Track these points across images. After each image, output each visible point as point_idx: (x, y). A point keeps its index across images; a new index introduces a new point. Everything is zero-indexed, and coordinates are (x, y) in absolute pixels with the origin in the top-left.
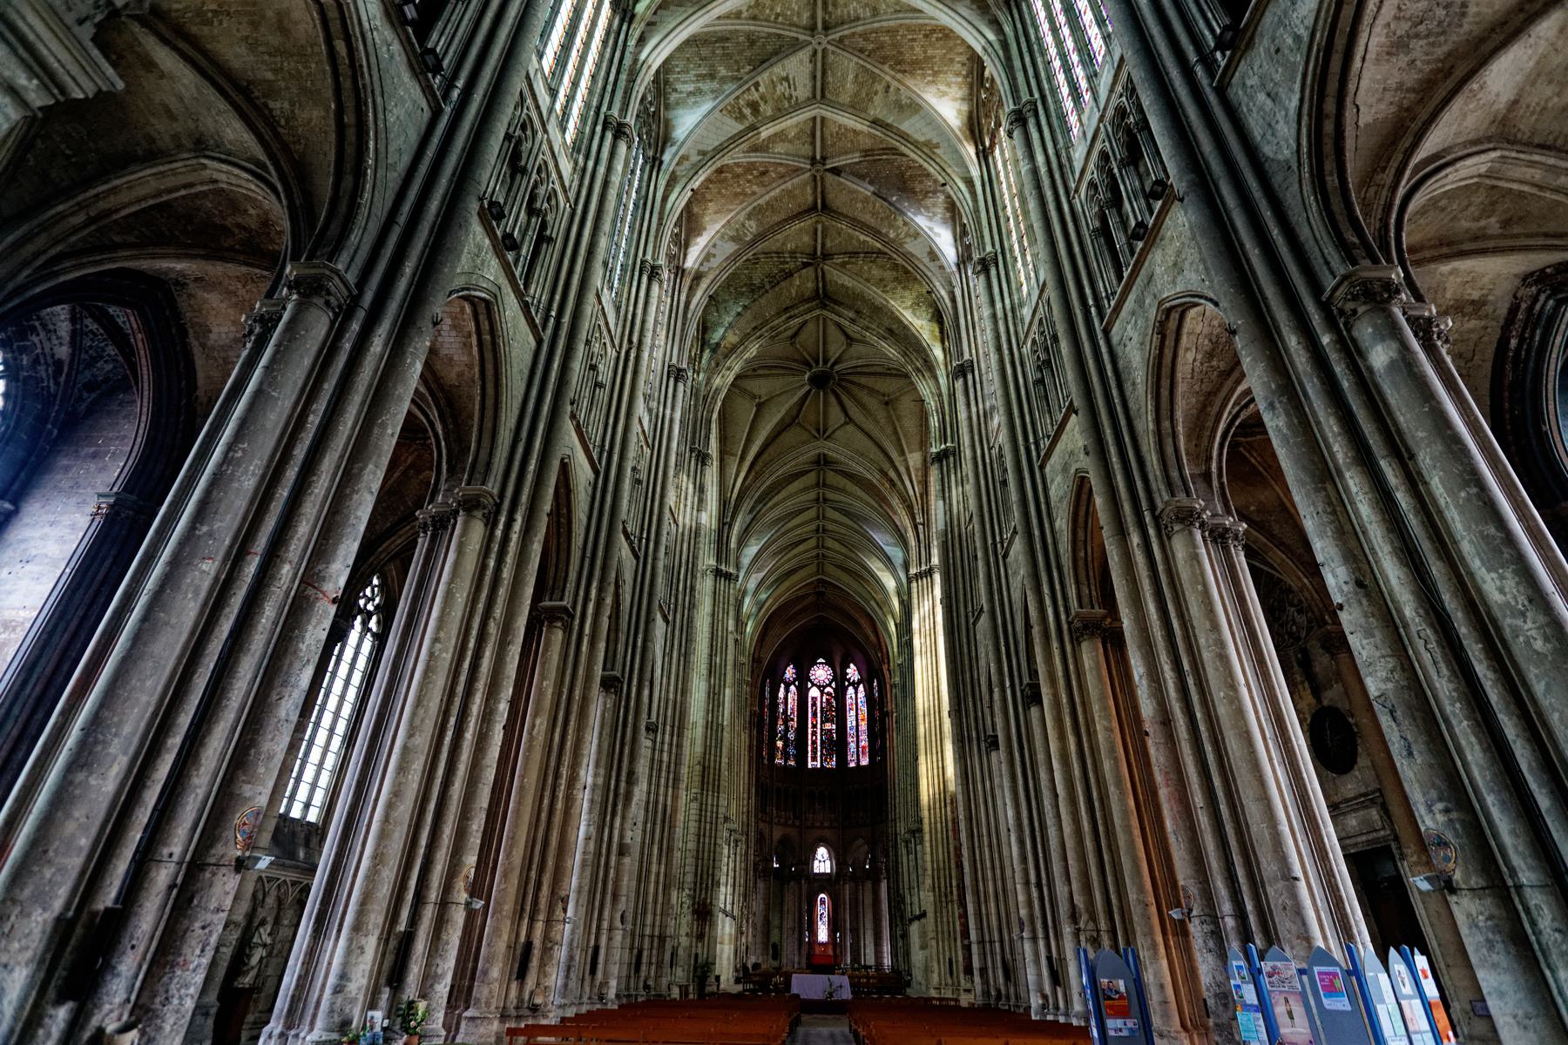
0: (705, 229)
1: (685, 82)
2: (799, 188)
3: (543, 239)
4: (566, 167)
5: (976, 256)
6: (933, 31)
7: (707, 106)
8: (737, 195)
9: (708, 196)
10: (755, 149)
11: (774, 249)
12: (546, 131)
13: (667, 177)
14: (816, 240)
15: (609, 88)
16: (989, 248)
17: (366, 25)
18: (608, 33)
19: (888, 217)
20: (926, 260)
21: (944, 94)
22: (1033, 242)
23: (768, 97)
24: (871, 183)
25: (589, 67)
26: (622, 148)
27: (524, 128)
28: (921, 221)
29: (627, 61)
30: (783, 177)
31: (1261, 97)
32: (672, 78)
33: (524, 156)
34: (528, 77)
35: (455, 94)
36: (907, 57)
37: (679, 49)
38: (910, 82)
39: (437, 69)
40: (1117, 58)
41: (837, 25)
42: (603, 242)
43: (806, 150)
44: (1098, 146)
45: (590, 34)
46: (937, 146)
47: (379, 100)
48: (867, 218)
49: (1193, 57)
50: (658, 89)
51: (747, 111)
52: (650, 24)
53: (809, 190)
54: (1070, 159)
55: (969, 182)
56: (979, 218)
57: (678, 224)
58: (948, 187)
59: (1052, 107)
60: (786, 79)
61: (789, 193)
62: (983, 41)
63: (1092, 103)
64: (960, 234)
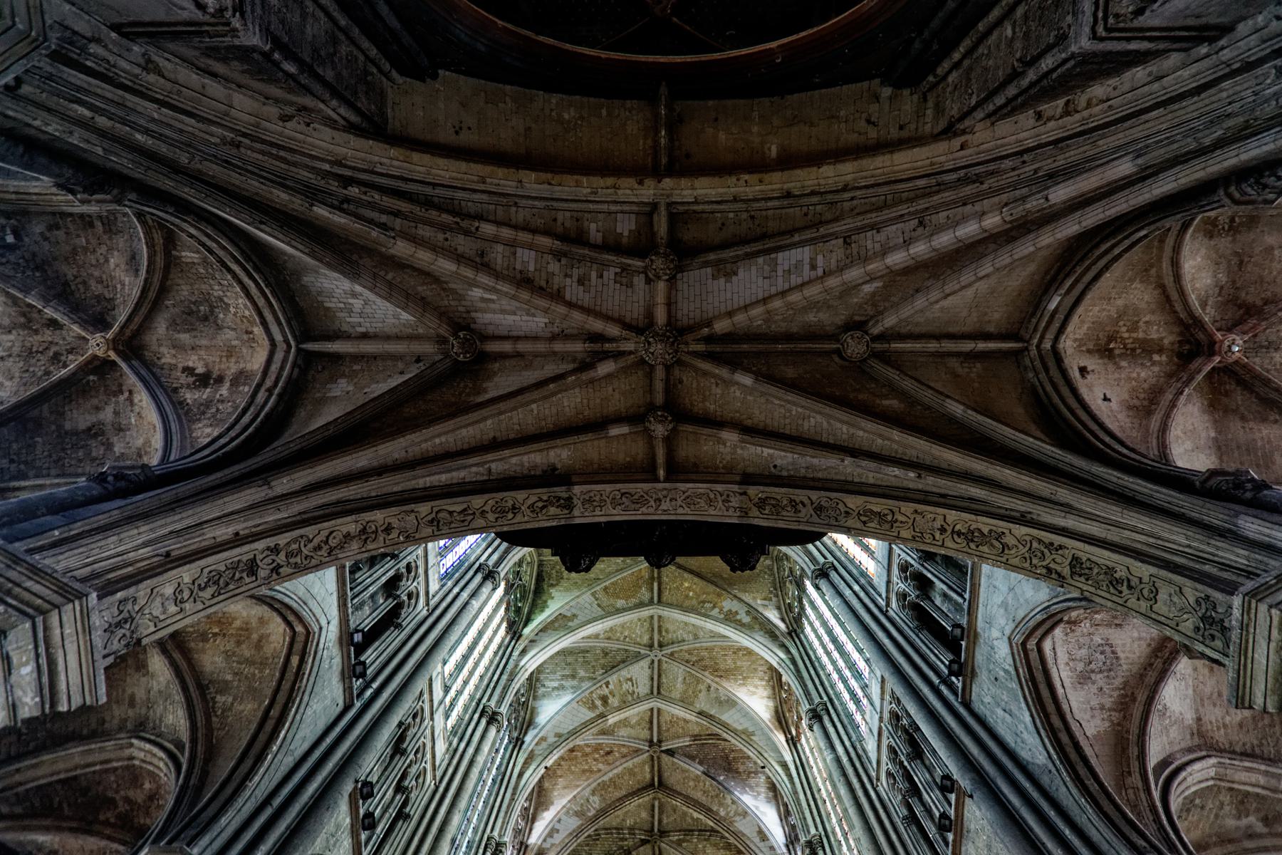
0: (552, 803)
1: (553, 680)
2: (640, 768)
3: (402, 815)
4: (441, 747)
5: (803, 839)
6: (739, 649)
7: (567, 697)
8: (584, 771)
9: (559, 773)
10: (603, 732)
11: (614, 824)
12: (432, 719)
13: (526, 756)
14: (653, 816)
15: (492, 685)
16: (813, 831)
17: (321, 646)
18: (499, 648)
19: (717, 796)
20: (757, 840)
21: (754, 693)
22: (852, 827)
23: (616, 692)
24: (701, 763)
25: (480, 670)
26: (493, 731)
27: (415, 716)
28: (747, 799)
29: (510, 667)
30: (624, 756)
31: (1000, 712)
32: (542, 677)
33: (408, 739)
34: (431, 680)
35: (369, 693)
36: (722, 666)
37: (552, 657)
38: (725, 684)
39: (363, 675)
40: (879, 674)
41: (668, 644)
42: (456, 819)
43: (645, 734)
44: (885, 742)
45: (486, 648)
46: (753, 734)
47: (306, 698)
48: (698, 795)
49: (936, 681)
50: (530, 685)
51: (598, 703)
52: (532, 641)
53: (647, 768)
54: (864, 750)
55: (784, 766)
56: (798, 799)
57: (529, 799)
58: (766, 770)
59: (839, 708)
60: (631, 680)
61: (631, 772)
62: (777, 659)
63: (869, 707)
64: (785, 815)
